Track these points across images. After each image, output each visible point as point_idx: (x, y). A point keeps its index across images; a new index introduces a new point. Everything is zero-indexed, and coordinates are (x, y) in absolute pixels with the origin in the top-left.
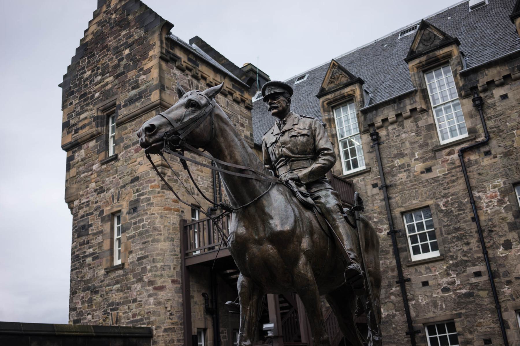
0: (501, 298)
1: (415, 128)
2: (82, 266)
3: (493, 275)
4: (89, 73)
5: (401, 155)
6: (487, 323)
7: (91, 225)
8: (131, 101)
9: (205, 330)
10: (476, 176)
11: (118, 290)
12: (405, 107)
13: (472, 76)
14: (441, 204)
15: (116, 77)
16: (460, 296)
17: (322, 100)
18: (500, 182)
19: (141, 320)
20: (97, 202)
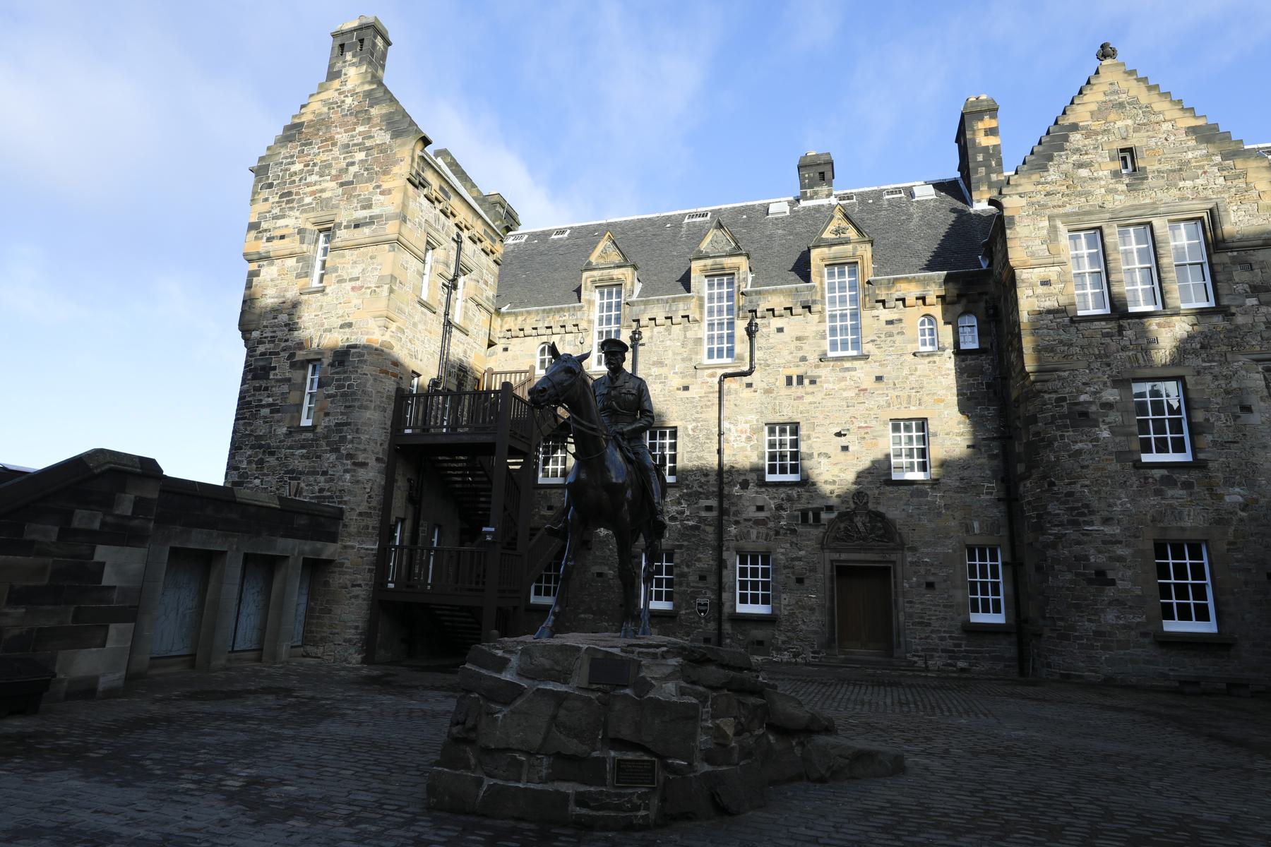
0: (726, 537)
1: (682, 338)
2: (255, 416)
3: (723, 512)
4: (297, 167)
5: (660, 363)
6: (706, 560)
7: (274, 368)
9: (403, 520)
10: (732, 406)
11: (302, 456)
12: (677, 311)
13: (754, 297)
14: (690, 427)
16: (686, 528)
17: (585, 275)
18: (753, 417)
19: (331, 497)
20: (286, 341)
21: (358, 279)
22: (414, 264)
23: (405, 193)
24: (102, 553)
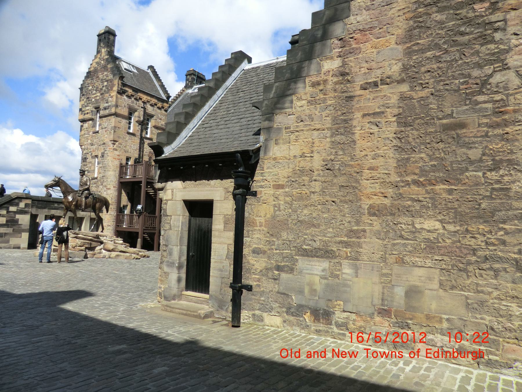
4: (91, 88)
8: (105, 109)
15: (101, 94)
21: (106, 128)
22: (124, 122)
23: (117, 97)
24: (18, 216)
